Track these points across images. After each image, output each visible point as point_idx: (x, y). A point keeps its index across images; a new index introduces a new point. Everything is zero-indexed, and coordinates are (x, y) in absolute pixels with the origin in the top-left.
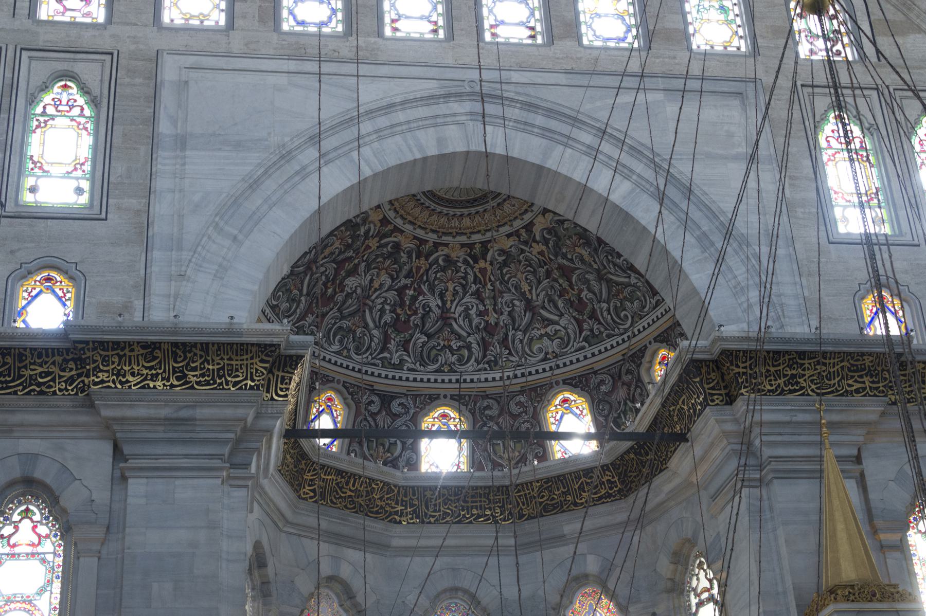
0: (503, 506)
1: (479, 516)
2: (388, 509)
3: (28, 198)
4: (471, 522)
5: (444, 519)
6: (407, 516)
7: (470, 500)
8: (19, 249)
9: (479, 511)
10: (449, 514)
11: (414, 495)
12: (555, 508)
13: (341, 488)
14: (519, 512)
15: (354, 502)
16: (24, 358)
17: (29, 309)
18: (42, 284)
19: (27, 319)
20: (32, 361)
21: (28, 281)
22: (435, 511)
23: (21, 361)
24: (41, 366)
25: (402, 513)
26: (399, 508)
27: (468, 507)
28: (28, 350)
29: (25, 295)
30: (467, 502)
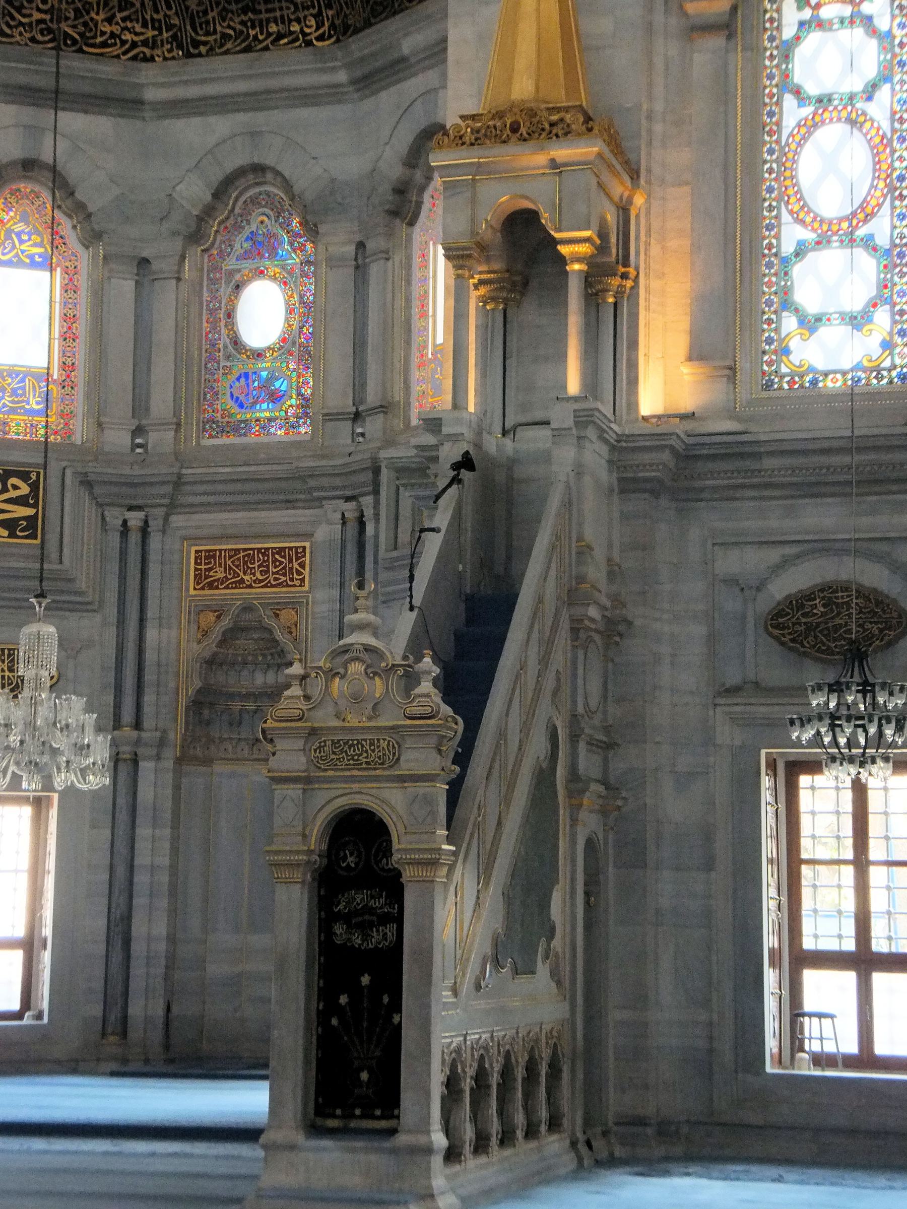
0: (320, 13)
1: (280, 36)
2: (127, 36)
4: (266, 48)
5: (222, 45)
6: (162, 45)
7: (262, 7)
9: (281, 26)
10: (230, 36)
11: (169, 7)
12: (385, 8)
13: (19, 10)
14: (343, 21)
15: (50, 31)
22: (208, 34)
25: (154, 42)
26: (150, 33)
27: (261, 21)
30: (260, 12)
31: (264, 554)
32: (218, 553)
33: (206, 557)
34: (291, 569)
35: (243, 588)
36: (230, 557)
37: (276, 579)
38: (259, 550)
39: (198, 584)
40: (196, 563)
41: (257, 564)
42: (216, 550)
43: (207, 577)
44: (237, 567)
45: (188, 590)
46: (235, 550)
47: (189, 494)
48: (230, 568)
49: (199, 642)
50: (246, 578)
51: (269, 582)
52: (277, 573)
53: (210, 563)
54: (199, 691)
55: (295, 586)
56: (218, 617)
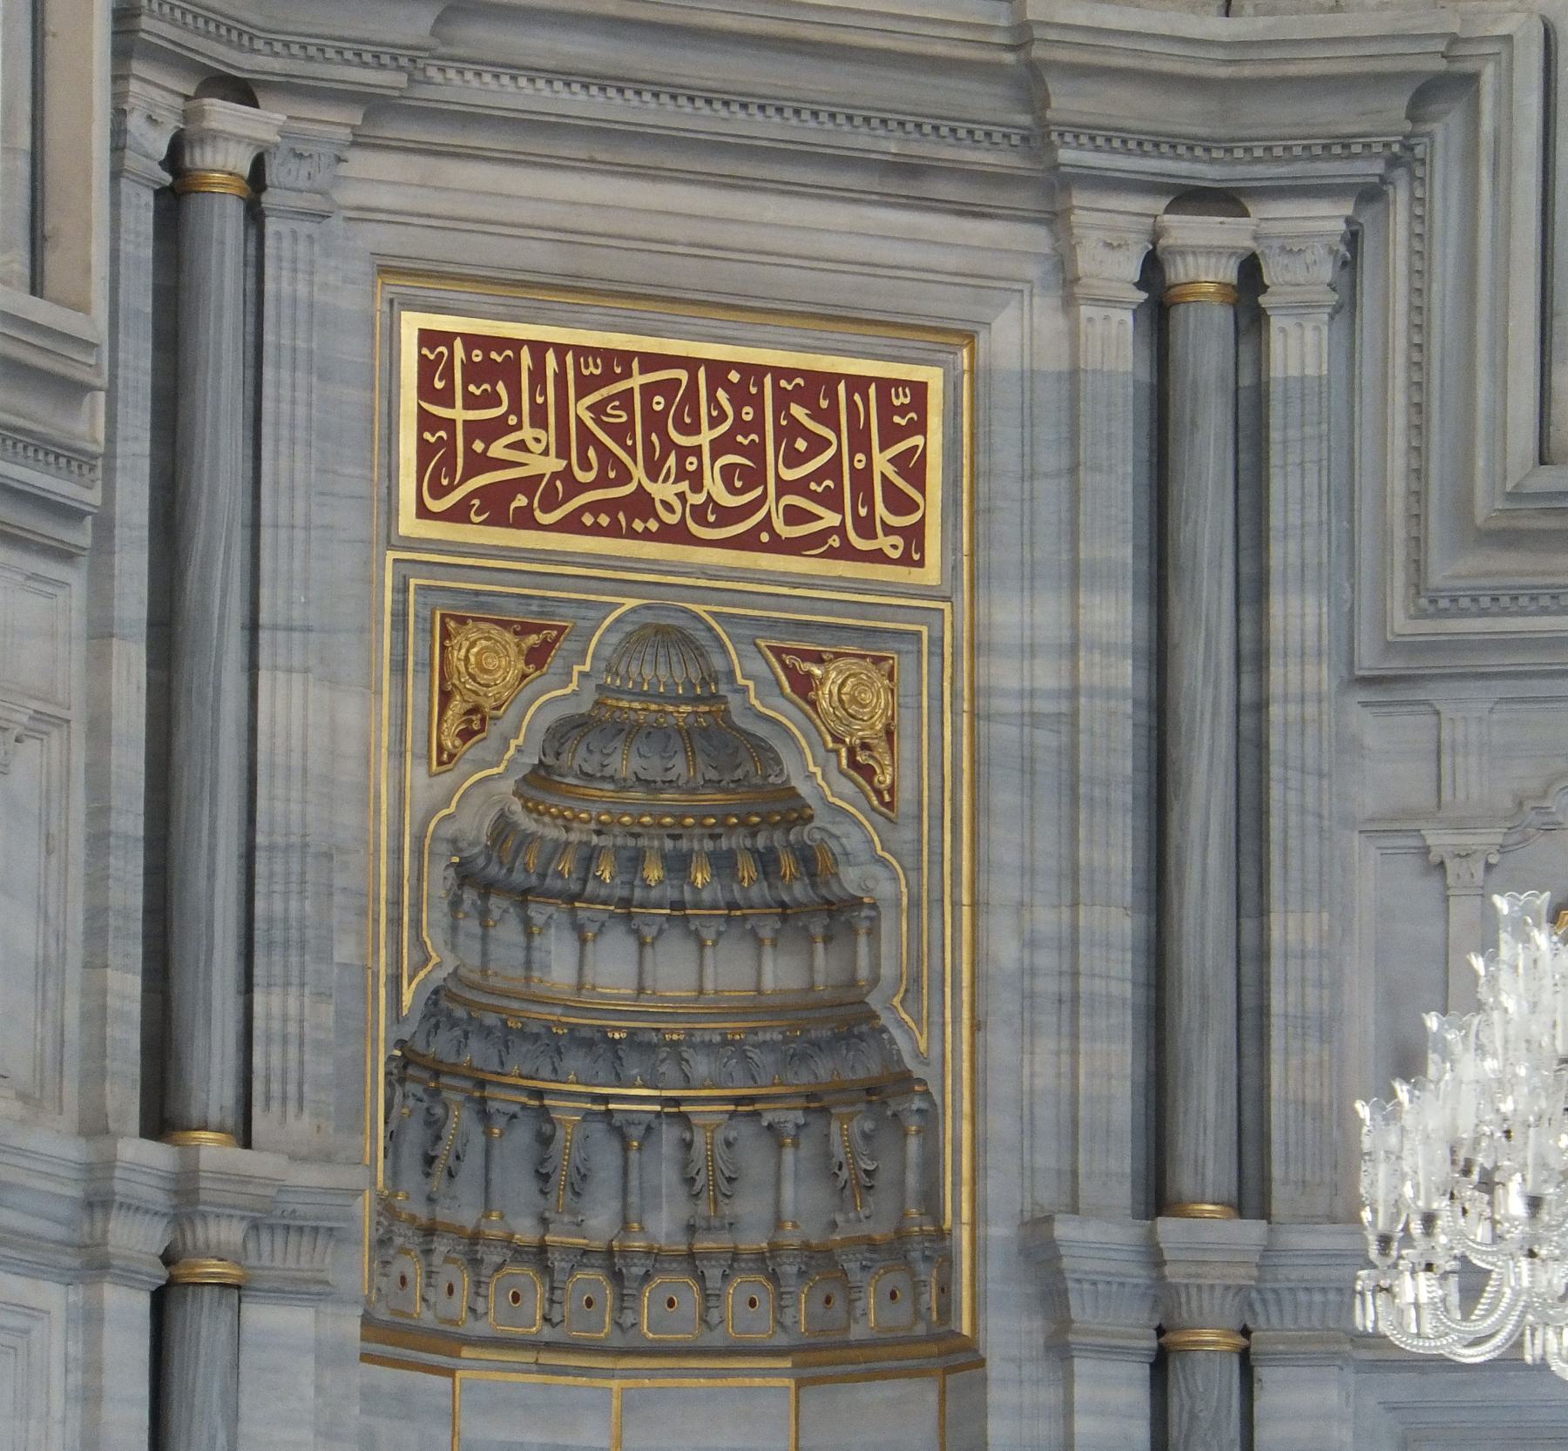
31: (740, 396)
32: (525, 355)
33: (473, 373)
34: (863, 479)
35: (647, 536)
36: (586, 386)
37: (795, 516)
38: (717, 370)
39: (438, 492)
40: (426, 390)
41: (705, 437)
42: (516, 344)
43: (479, 464)
44: (620, 433)
45: (392, 512)
46: (607, 355)
47: (479, 64)
48: (586, 437)
49: (447, 759)
50: (663, 491)
51: (766, 524)
52: (800, 487)
53: (492, 400)
54: (437, 1004)
55: (878, 557)
56: (537, 657)
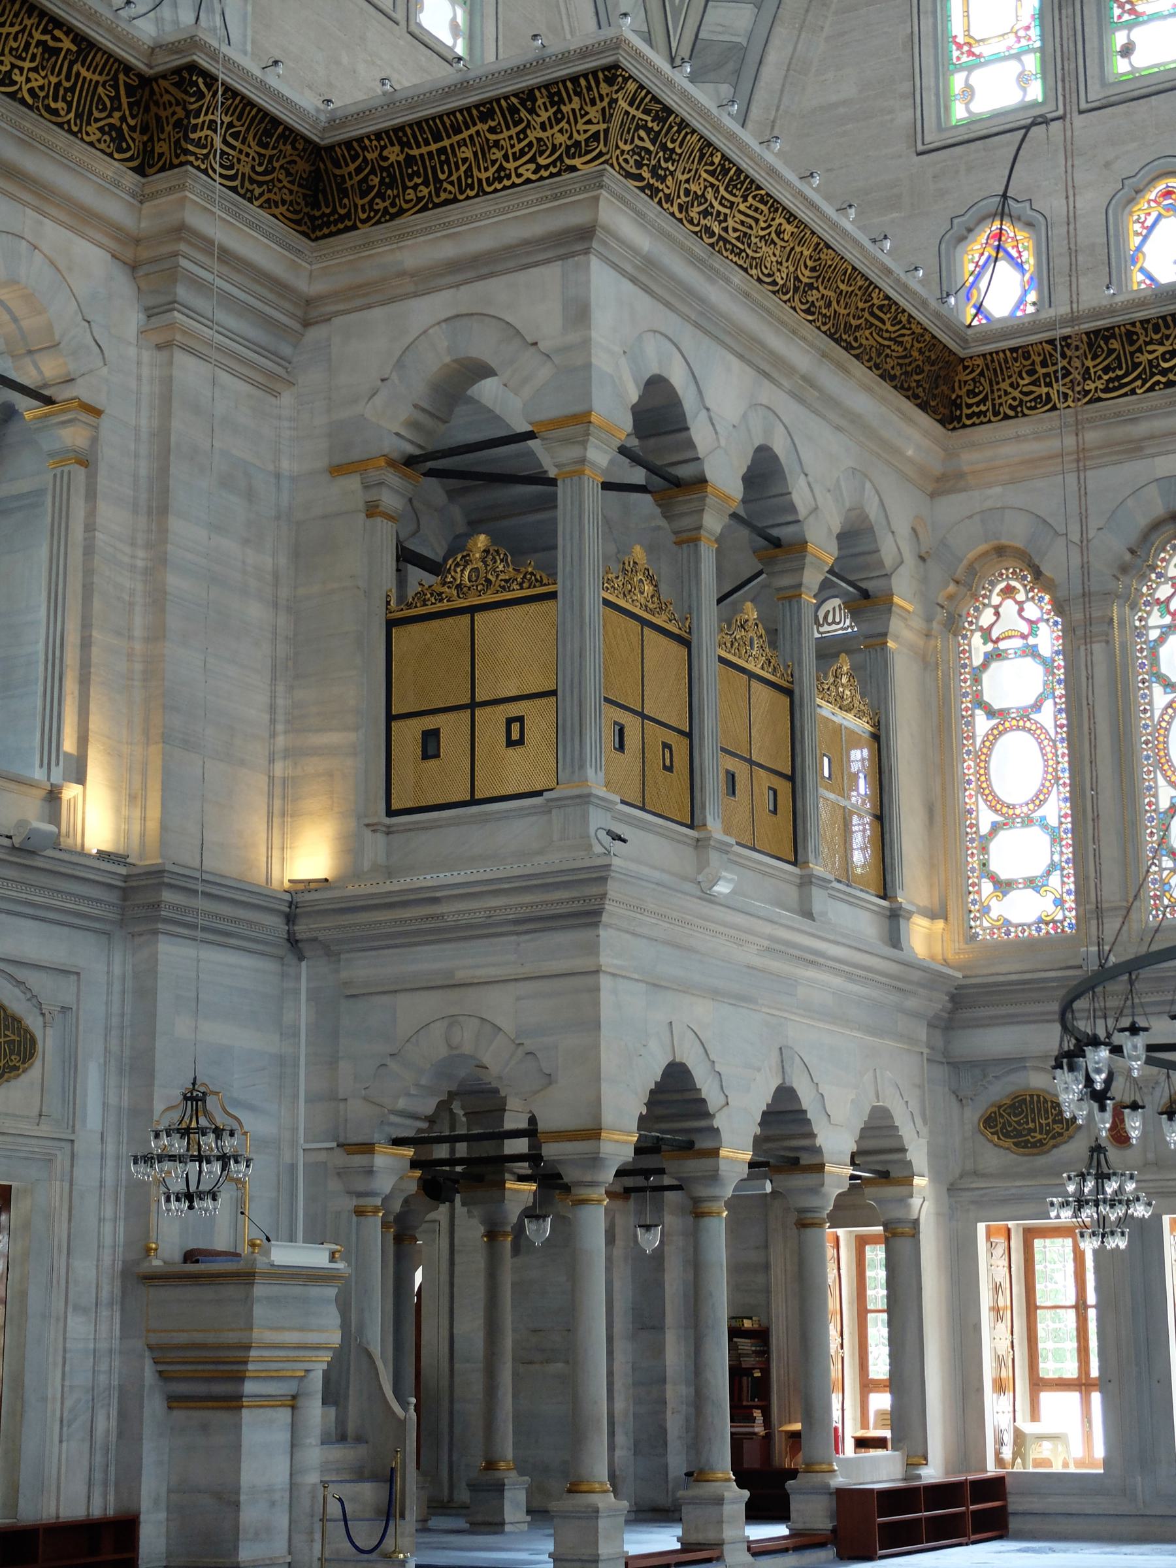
3: (1122, 66)
8: (1117, 158)
16: (1135, 337)
17: (1145, 249)
18: (1159, 204)
19: (1146, 265)
20: (1148, 339)
21: (1138, 203)
23: (1132, 343)
24: (1162, 344)
28: (1138, 324)
29: (1137, 227)
